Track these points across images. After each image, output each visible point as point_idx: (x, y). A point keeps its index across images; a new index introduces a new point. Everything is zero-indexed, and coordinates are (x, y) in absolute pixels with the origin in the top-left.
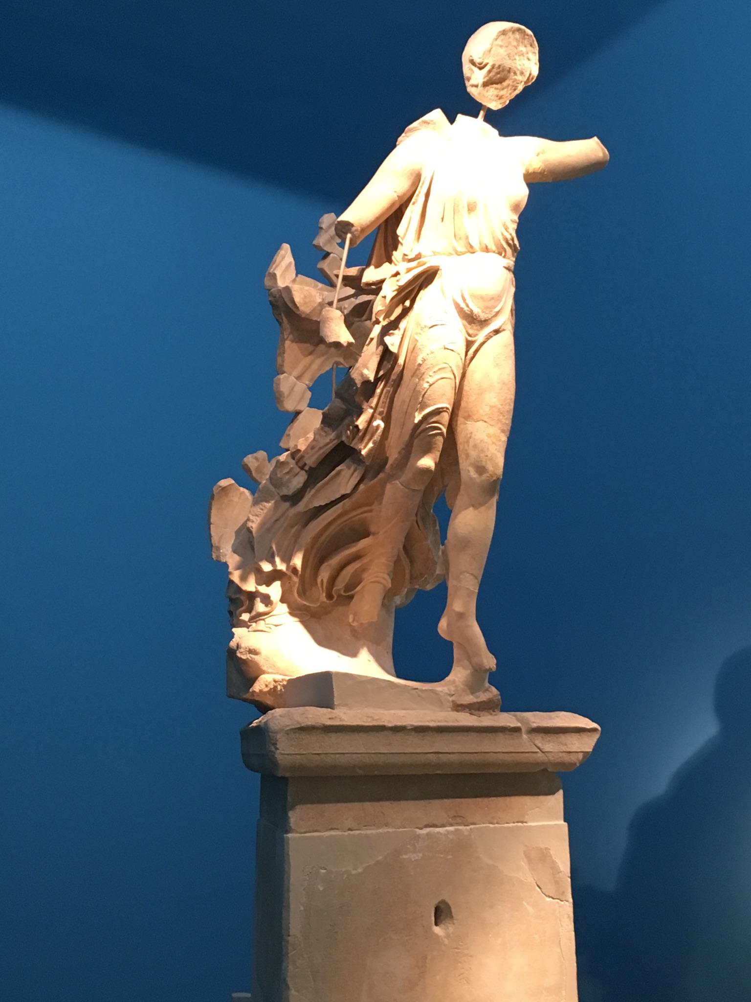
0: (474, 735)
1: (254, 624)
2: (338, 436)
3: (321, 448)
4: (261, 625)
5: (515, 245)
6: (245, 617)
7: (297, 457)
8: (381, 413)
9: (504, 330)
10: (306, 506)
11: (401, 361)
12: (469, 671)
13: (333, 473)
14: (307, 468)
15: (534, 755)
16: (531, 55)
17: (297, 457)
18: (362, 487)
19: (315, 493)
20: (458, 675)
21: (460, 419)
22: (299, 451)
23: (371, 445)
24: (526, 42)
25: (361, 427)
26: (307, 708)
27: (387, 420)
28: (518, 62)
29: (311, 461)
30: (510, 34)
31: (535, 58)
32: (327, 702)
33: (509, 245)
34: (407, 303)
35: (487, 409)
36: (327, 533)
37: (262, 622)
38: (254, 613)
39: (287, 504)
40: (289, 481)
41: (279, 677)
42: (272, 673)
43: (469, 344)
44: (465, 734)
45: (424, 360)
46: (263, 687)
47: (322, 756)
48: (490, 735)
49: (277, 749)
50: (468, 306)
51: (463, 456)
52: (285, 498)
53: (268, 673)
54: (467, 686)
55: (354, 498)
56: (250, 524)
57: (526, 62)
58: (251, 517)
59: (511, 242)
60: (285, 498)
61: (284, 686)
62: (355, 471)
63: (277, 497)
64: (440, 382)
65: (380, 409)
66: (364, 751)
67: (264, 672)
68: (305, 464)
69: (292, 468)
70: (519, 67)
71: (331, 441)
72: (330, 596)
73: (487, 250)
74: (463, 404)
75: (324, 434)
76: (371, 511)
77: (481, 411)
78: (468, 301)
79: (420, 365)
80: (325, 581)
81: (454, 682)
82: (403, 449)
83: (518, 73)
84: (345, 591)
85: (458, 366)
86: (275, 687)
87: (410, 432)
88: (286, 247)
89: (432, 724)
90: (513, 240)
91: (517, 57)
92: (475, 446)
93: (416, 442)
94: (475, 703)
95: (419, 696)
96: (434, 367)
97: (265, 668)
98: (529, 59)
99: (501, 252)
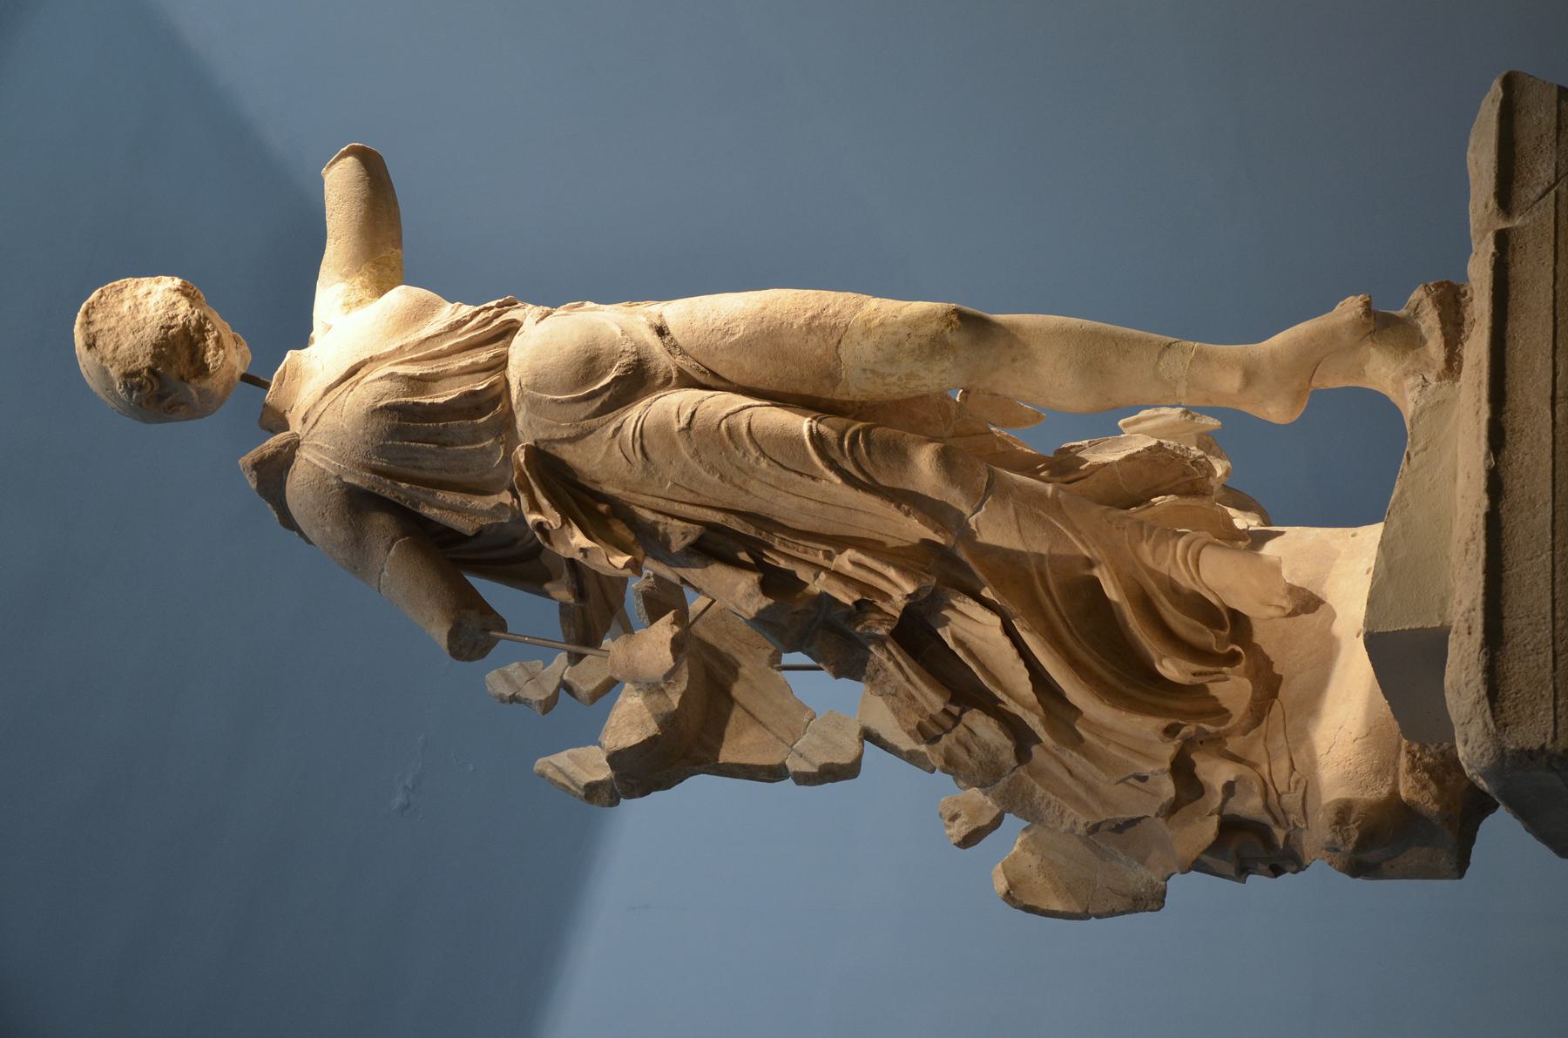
0: (1511, 326)
1: (1292, 817)
2: (880, 642)
3: (908, 679)
4: (1291, 800)
5: (499, 306)
6: (1280, 835)
7: (936, 731)
8: (829, 556)
10: (1031, 709)
11: (718, 518)
12: (1372, 350)
13: (960, 653)
14: (955, 710)
15: (1563, 198)
17: (936, 731)
18: (987, 593)
19: (1005, 691)
20: (1382, 371)
21: (839, 394)
22: (920, 727)
23: (892, 573)
25: (857, 597)
26: (1447, 683)
27: (842, 542)
29: (934, 701)
31: (147, 283)
32: (1434, 644)
33: (497, 316)
34: (603, 508)
35: (814, 340)
36: (1097, 668)
37: (1285, 799)
38: (1267, 819)
39: (1035, 749)
40: (985, 747)
41: (1404, 762)
42: (1396, 776)
44: (1509, 344)
45: (712, 469)
46: (1426, 795)
47: (1560, 647)
48: (1513, 293)
49: (1543, 747)
51: (912, 384)
52: (1022, 755)
53: (1395, 783)
54: (1405, 353)
55: (1011, 608)
56: (1081, 829)
57: (152, 300)
58: (1066, 826)
60: (1022, 755)
61: (1423, 748)
62: (953, 608)
63: (1022, 771)
65: (820, 558)
66: (1546, 556)
67: (1394, 793)
68: (945, 711)
69: (958, 741)
70: (161, 312)
71: (891, 657)
72: (1233, 659)
74: (807, 390)
75: (881, 675)
76: (1042, 576)
77: (819, 352)
79: (721, 477)
80: (1196, 668)
81: (1397, 382)
82: (899, 507)
84: (1222, 628)
86: (1426, 768)
87: (861, 493)
88: (540, 764)
89: (1485, 414)
91: (141, 317)
92: (892, 361)
93: (882, 482)
94: (1444, 334)
96: (725, 449)
97: (1385, 791)
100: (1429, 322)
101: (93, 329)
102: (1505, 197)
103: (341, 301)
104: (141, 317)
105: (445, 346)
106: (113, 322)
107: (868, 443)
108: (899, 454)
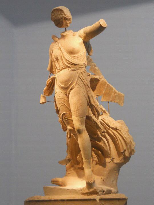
0: (80, 201)
9: (74, 88)
16: (62, 13)
24: (59, 11)
28: (59, 17)
30: (54, 12)
33: (71, 64)
43: (66, 94)
50: (61, 85)
59: (71, 63)
64: (61, 107)
73: (64, 69)
78: (61, 84)
83: (61, 19)
85: (64, 102)
90: (71, 62)
91: (58, 16)
95: (70, 191)
98: (62, 14)
99: (69, 67)
100: (91, 190)
101: (54, 12)
102: (100, 200)
103: (80, 34)
104: (58, 16)
105: (64, 60)
106: (56, 13)
107: (67, 120)
108: (68, 124)
